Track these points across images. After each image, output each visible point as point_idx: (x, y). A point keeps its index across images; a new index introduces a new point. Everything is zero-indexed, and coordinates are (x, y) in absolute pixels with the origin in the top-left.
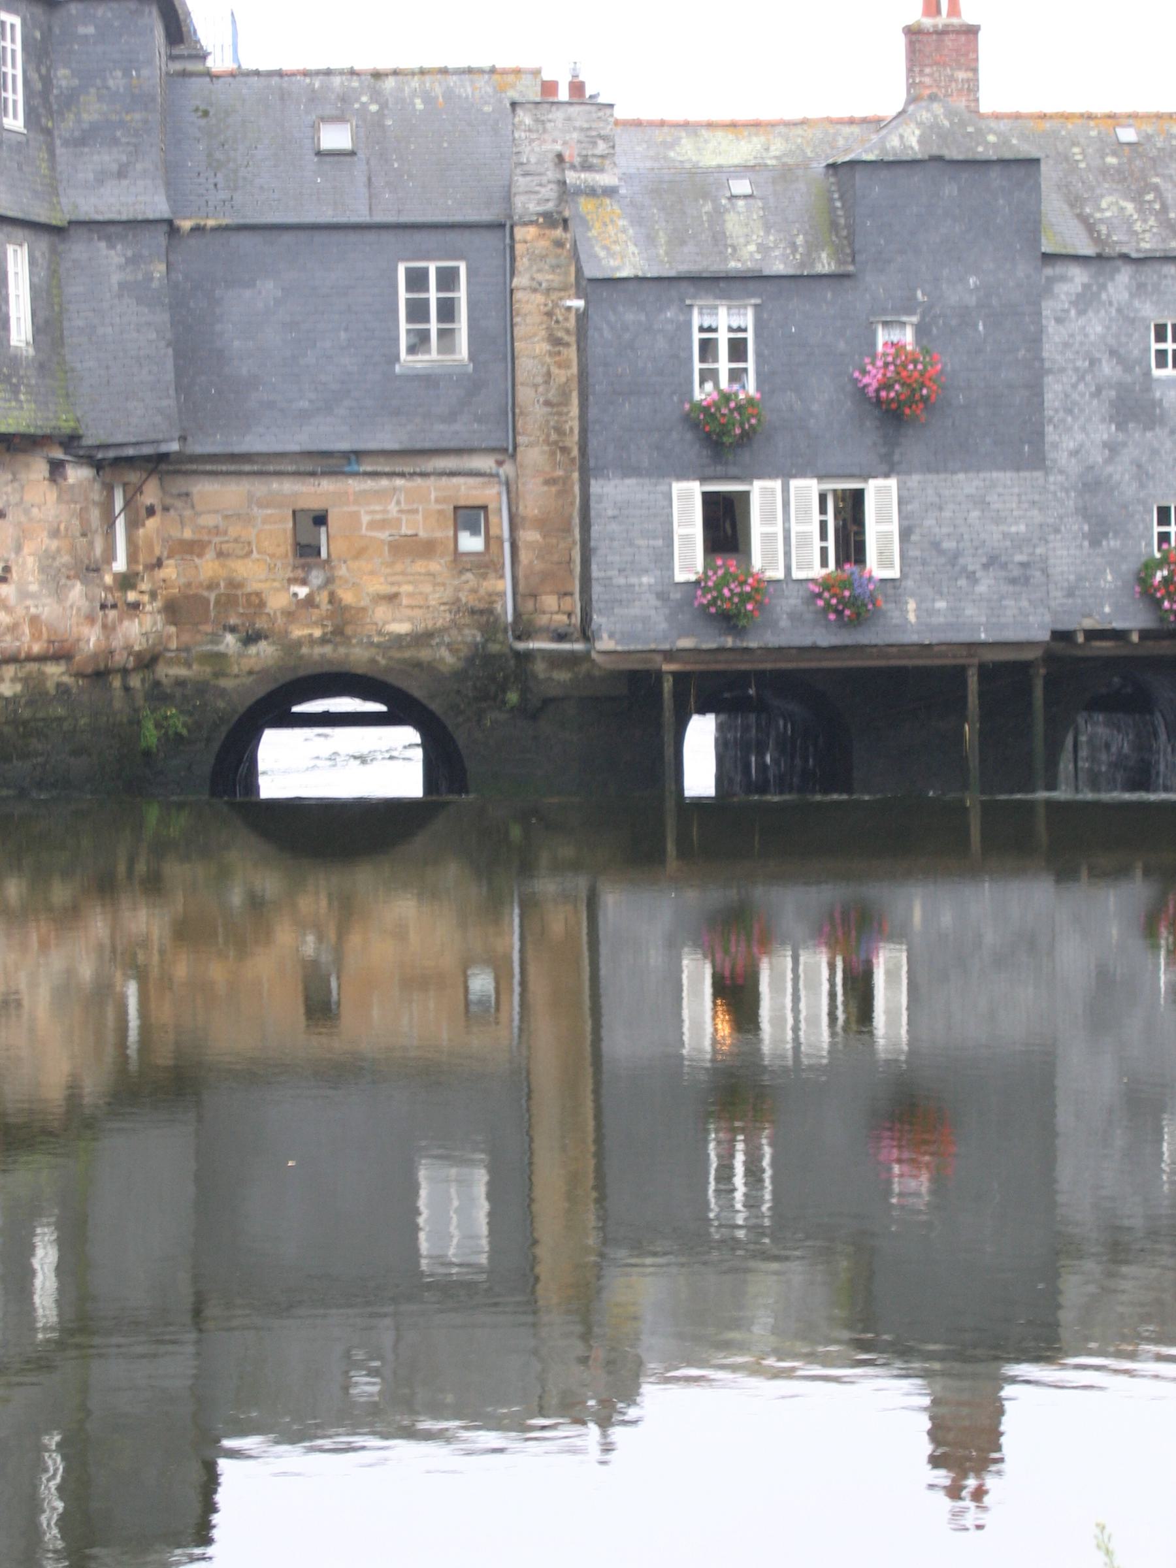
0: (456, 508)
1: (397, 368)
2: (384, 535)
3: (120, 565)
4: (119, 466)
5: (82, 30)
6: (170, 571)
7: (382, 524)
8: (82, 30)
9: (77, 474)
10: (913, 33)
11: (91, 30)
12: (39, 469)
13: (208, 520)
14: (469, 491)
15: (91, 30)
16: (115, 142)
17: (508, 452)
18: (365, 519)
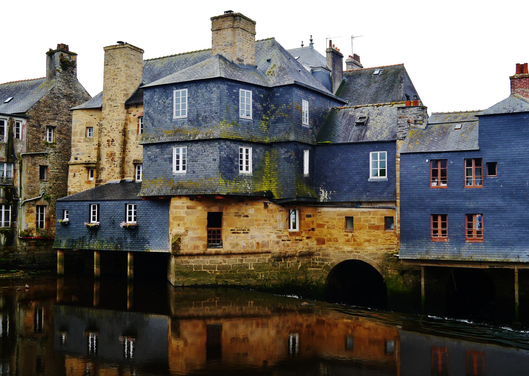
0: (386, 218)
1: (369, 180)
2: (367, 224)
3: (297, 230)
4: (287, 205)
5: (277, 95)
6: (316, 232)
7: (367, 221)
8: (277, 95)
9: (271, 206)
10: (512, 78)
11: (279, 94)
12: (261, 206)
13: (326, 219)
14: (388, 213)
15: (279, 94)
16: (283, 122)
17: (395, 202)
18: (362, 220)
